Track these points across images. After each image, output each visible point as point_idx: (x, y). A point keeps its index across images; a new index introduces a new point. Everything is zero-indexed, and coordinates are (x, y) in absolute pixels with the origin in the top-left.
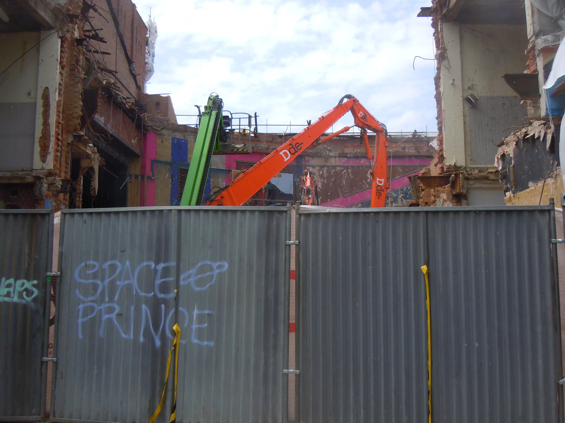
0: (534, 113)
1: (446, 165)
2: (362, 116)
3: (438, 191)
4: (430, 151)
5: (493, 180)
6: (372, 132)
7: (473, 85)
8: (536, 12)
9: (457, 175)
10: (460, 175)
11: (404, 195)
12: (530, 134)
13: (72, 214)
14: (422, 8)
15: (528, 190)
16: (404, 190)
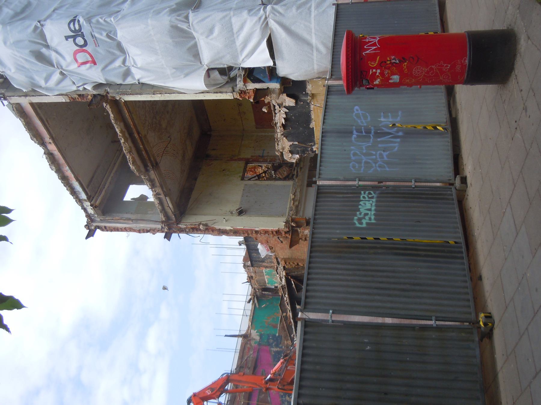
1: (284, 228)
2: (211, 391)
3: (302, 236)
4: (249, 366)
5: (299, 203)
6: (227, 386)
8: (221, 90)
9: (293, 220)
11: (287, 395)
12: (282, 122)
13: (320, 174)
14: (165, 238)
15: (314, 129)
16: (282, 394)
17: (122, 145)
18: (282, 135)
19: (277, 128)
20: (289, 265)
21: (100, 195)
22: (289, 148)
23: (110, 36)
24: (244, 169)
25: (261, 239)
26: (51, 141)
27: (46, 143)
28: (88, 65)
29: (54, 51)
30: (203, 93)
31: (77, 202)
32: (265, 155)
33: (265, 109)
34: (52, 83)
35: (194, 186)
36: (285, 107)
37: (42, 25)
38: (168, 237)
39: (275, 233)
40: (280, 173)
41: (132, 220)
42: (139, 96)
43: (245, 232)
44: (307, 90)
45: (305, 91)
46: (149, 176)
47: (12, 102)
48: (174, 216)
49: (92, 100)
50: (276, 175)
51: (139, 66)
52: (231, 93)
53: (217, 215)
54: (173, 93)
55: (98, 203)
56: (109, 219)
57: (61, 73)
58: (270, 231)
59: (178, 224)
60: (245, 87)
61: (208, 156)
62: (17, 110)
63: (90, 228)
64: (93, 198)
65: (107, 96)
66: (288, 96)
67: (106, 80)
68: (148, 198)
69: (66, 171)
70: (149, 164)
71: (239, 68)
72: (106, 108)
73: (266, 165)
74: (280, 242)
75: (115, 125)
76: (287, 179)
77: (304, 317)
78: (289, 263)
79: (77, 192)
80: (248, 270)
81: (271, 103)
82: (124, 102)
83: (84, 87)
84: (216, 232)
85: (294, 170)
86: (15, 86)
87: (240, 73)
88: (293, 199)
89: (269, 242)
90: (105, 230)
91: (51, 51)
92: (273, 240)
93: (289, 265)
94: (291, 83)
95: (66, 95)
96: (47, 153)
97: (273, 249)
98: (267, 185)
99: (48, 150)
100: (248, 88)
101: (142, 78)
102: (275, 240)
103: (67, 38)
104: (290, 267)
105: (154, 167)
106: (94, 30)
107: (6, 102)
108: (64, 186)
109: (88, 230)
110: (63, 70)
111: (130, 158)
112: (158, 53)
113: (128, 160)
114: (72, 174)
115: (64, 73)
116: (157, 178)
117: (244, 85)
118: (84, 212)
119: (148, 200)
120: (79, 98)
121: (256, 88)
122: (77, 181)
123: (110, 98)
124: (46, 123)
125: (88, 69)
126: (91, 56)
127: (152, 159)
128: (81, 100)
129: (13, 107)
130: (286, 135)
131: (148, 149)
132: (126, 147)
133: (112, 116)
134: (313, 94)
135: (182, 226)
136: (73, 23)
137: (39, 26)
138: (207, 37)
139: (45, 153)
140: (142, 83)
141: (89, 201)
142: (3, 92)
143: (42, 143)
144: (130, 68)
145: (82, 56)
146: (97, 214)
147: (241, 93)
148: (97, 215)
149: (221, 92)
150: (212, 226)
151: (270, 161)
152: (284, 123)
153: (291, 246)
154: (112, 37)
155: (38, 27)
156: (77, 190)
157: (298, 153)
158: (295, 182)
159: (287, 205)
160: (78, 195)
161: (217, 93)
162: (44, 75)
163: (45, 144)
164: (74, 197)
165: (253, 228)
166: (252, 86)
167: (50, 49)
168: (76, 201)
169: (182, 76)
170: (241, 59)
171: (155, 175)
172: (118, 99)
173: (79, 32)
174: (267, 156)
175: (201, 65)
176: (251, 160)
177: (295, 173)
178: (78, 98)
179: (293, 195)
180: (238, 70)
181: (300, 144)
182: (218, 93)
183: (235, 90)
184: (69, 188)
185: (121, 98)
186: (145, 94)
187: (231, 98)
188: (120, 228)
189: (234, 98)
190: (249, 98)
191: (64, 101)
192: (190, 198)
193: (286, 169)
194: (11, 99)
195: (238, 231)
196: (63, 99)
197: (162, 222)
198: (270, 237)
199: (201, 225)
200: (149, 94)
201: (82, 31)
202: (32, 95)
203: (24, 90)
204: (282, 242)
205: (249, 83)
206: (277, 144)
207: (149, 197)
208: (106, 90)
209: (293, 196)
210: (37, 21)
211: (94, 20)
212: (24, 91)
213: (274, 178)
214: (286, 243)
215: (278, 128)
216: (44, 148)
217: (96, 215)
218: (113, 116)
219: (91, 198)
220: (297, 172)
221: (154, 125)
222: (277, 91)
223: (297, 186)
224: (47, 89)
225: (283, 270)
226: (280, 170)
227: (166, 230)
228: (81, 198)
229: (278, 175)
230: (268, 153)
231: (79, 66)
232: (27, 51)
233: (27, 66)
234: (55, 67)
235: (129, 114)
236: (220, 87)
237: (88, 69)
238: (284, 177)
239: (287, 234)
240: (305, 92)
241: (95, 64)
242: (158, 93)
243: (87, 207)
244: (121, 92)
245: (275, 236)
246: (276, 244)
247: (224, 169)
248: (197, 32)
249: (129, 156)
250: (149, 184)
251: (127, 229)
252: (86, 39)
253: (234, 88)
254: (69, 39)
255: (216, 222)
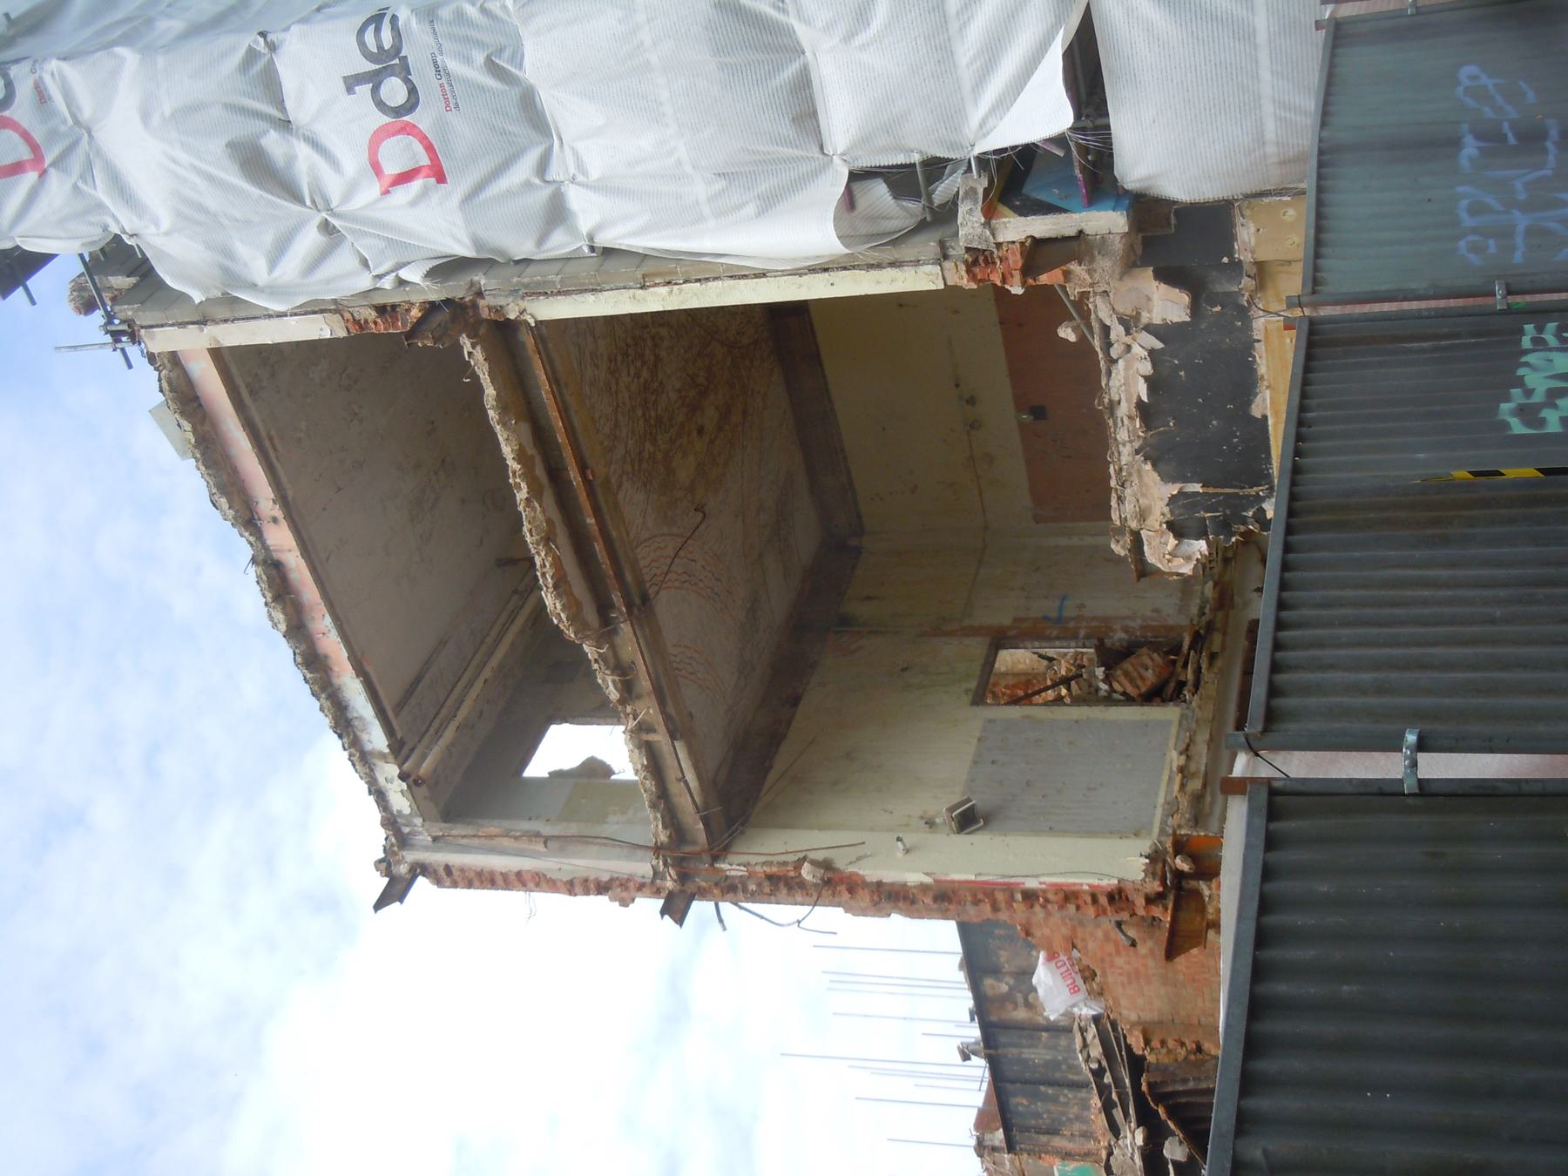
0: (1111, 259)
1: (1144, 880)
5: (1205, 785)
7: (922, 818)
9: (1180, 846)
10: (1181, 835)
12: (1139, 397)
15: (1270, 422)
17: (521, 508)
18: (1137, 452)
19: (1115, 424)
20: (1164, 1051)
21: (438, 740)
22: (1166, 510)
23: (498, 65)
24: (984, 665)
25: (1046, 931)
26: (278, 512)
27: (260, 520)
28: (417, 185)
29: (305, 140)
30: (826, 270)
31: (354, 765)
32: (1067, 613)
33: (1069, 330)
34: (290, 267)
35: (789, 724)
36: (1150, 329)
37: (273, 47)
38: (675, 909)
39: (1103, 900)
40: (1126, 674)
41: (546, 841)
42: (590, 297)
43: (980, 896)
44: (1236, 247)
45: (1231, 255)
46: (613, 647)
47: (155, 348)
48: (701, 826)
49: (421, 321)
50: (1111, 685)
51: (595, 174)
52: (933, 264)
53: (872, 829)
54: (715, 279)
55: (426, 767)
56: (463, 833)
57: (326, 228)
58: (1084, 892)
59: (715, 858)
60: (988, 233)
61: (845, 621)
62: (171, 391)
63: (394, 870)
64: (412, 750)
65: (474, 306)
66: (1165, 276)
67: (477, 243)
68: (614, 773)
69: (324, 634)
70: (616, 597)
71: (970, 160)
72: (472, 363)
73: (1072, 650)
74: (1127, 943)
75: (498, 427)
76: (1158, 699)
77: (1265, 772)
78: (1163, 1043)
79: (356, 723)
80: (994, 1164)
81: (1093, 316)
82: (533, 325)
83: (397, 275)
84: (865, 897)
85: (1185, 665)
86: (169, 281)
87: (971, 184)
88: (1182, 770)
89: (1079, 946)
90: (448, 881)
91: (294, 141)
92: (1099, 933)
93: (1164, 1051)
94: (1173, 221)
95: (337, 308)
96: (261, 558)
97: (1098, 979)
98: (1076, 722)
99: (265, 547)
100: (1000, 240)
101: (600, 227)
102: (1107, 938)
103: (351, 83)
104: (1166, 1061)
105: (636, 611)
106: (446, 45)
107: (133, 351)
108: (313, 694)
109: (387, 880)
110: (330, 215)
111: (547, 565)
112: (664, 115)
113: (538, 574)
114: (341, 645)
115: (334, 227)
116: (644, 661)
117: (987, 224)
118: (375, 805)
119: (613, 777)
120: (379, 320)
121: (1033, 237)
122: (358, 676)
123: (485, 314)
124: (267, 444)
125: (414, 203)
126: (429, 148)
127: (629, 577)
128: (385, 329)
129: (160, 380)
130: (1155, 454)
131: (614, 534)
132: (534, 517)
133: (490, 392)
134: (1260, 266)
135: (732, 867)
136: (374, 25)
137: (263, 51)
138: (848, 38)
139: (254, 560)
140: (605, 249)
141: (396, 758)
142: (130, 313)
143: (248, 521)
144: (563, 189)
145: (399, 154)
146: (422, 815)
147: (975, 262)
148: (421, 820)
149: (894, 264)
150: (851, 869)
151: (1087, 637)
152: (1145, 399)
153: (1172, 952)
154: (503, 67)
155: (259, 52)
156: (357, 711)
157: (1202, 534)
158: (1188, 708)
159: (1156, 794)
160: (358, 733)
161: (879, 266)
162: (268, 238)
163: (259, 523)
164: (345, 740)
165: (1013, 880)
166: (1016, 228)
167: (291, 135)
168: (349, 759)
169: (751, 209)
170: (975, 117)
171: (637, 640)
172: (512, 316)
173: (394, 58)
174: (1079, 618)
175: (821, 156)
176: (1014, 632)
177: (1190, 676)
178: (375, 323)
179: (1181, 754)
180: (963, 174)
181: (1211, 490)
182: (885, 268)
183: (951, 252)
184: (329, 703)
185: (524, 310)
186: (612, 289)
187: (932, 287)
188: (501, 873)
189: (945, 284)
190: (1004, 281)
191: (327, 335)
192: (771, 767)
193: (1152, 660)
194: (152, 338)
195: (953, 892)
196: (324, 326)
197: (658, 849)
198: (1081, 924)
199: (806, 864)
200: (625, 288)
201: (403, 54)
202: (223, 316)
203: (198, 297)
204: (1134, 944)
205: (1006, 217)
206: (1119, 498)
207: (615, 768)
208: (472, 284)
209: (1183, 758)
210: (255, 33)
211: (445, 13)
212: (197, 301)
213: (1105, 697)
214: (1152, 952)
215: (1120, 424)
216: (252, 539)
217: (418, 821)
218: (495, 393)
219: (405, 750)
220: (1198, 671)
221: (645, 465)
222: (1118, 245)
223: (1197, 721)
224: (273, 291)
225: (1132, 1125)
226: (1127, 665)
227: (669, 884)
228: (368, 747)
229: (1118, 682)
230: (1082, 606)
231: (386, 192)
232: (217, 146)
233: (213, 201)
234: (305, 205)
235: (550, 387)
236: (893, 243)
237: (414, 203)
238: (1143, 689)
239: (1153, 907)
240: (1231, 256)
241: (441, 178)
242: (657, 282)
243: (389, 786)
244: (526, 286)
245: (1105, 912)
246: (1110, 955)
247: (906, 665)
248: (807, 22)
249: (543, 554)
250: (614, 681)
251: (526, 877)
252: (415, 82)
253: (948, 244)
254: (357, 88)
255: (868, 856)
